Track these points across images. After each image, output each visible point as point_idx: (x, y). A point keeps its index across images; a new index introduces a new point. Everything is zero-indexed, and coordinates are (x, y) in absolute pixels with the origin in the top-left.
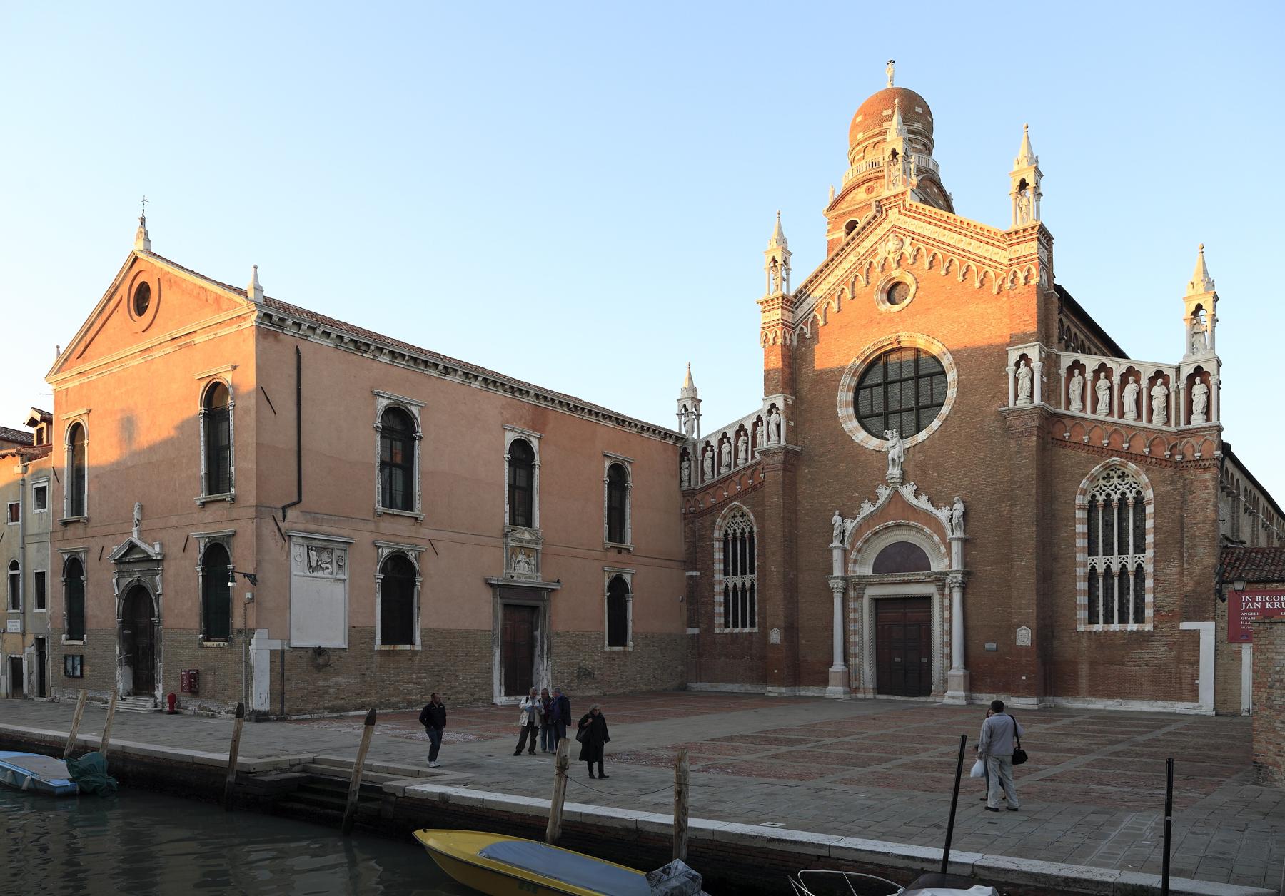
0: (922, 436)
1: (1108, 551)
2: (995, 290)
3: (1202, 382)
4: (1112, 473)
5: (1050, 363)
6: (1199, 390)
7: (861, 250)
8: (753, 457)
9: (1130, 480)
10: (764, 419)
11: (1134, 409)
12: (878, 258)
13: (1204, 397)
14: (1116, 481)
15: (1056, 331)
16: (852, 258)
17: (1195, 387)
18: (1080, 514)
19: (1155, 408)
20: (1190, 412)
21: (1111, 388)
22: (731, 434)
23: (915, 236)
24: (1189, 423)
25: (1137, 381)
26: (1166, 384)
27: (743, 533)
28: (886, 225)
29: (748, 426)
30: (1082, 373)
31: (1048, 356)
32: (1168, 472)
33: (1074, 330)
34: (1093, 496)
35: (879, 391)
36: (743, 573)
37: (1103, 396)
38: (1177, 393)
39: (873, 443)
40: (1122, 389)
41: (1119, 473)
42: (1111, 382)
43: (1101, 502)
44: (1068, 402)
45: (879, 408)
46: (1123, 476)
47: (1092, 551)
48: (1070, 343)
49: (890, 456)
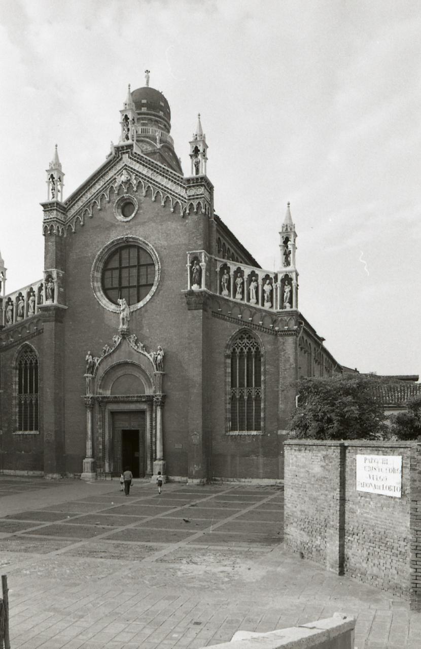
0: (141, 304)
2: (182, 214)
3: (288, 284)
4: (244, 336)
5: (211, 263)
7: (107, 178)
8: (38, 311)
10: (44, 285)
11: (255, 297)
12: (116, 185)
14: (246, 341)
15: (214, 244)
16: (101, 183)
19: (266, 297)
21: (243, 283)
22: (24, 294)
23: (138, 174)
27: (31, 363)
28: (121, 165)
29: (36, 289)
31: (210, 259)
33: (227, 246)
34: (234, 349)
35: (116, 273)
36: (31, 392)
38: (276, 289)
39: (112, 307)
40: (249, 284)
41: (247, 335)
43: (238, 353)
45: (116, 284)
46: (249, 338)
47: (233, 384)
48: (226, 254)
49: (121, 316)
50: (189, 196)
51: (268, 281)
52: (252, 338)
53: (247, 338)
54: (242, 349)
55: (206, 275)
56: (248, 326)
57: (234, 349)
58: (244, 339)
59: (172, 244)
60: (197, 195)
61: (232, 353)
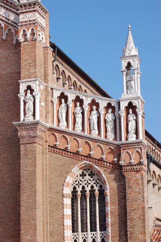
1: (84, 230)
2: (14, 42)
3: (133, 113)
4: (85, 172)
6: (131, 117)
9: (95, 177)
11: (96, 127)
13: (134, 122)
14: (87, 177)
17: (130, 116)
18: (68, 201)
20: (127, 132)
21: (83, 113)
24: (127, 139)
25: (97, 109)
26: (113, 112)
30: (66, 101)
32: (117, 172)
37: (79, 120)
41: (89, 172)
42: (83, 109)
44: (59, 121)
46: (91, 175)
50: (22, 22)
51: (110, 111)
52: (94, 175)
53: (89, 175)
54: (83, 187)
55: (41, 106)
56: (90, 161)
57: (75, 188)
58: (85, 175)
59: (4, 73)
60: (30, 21)
61: (72, 192)
